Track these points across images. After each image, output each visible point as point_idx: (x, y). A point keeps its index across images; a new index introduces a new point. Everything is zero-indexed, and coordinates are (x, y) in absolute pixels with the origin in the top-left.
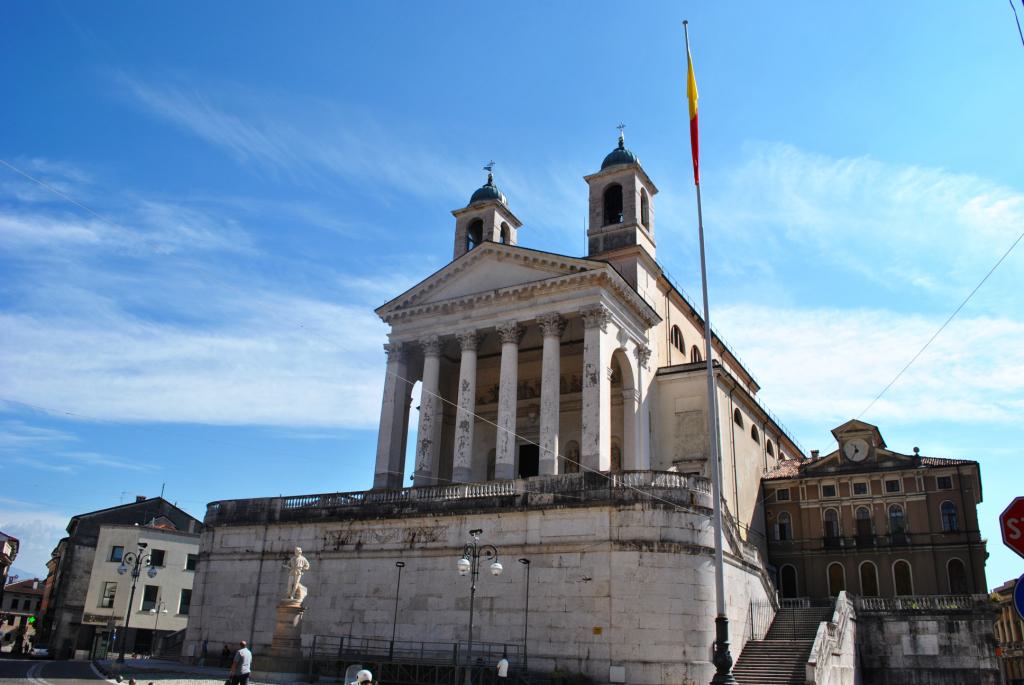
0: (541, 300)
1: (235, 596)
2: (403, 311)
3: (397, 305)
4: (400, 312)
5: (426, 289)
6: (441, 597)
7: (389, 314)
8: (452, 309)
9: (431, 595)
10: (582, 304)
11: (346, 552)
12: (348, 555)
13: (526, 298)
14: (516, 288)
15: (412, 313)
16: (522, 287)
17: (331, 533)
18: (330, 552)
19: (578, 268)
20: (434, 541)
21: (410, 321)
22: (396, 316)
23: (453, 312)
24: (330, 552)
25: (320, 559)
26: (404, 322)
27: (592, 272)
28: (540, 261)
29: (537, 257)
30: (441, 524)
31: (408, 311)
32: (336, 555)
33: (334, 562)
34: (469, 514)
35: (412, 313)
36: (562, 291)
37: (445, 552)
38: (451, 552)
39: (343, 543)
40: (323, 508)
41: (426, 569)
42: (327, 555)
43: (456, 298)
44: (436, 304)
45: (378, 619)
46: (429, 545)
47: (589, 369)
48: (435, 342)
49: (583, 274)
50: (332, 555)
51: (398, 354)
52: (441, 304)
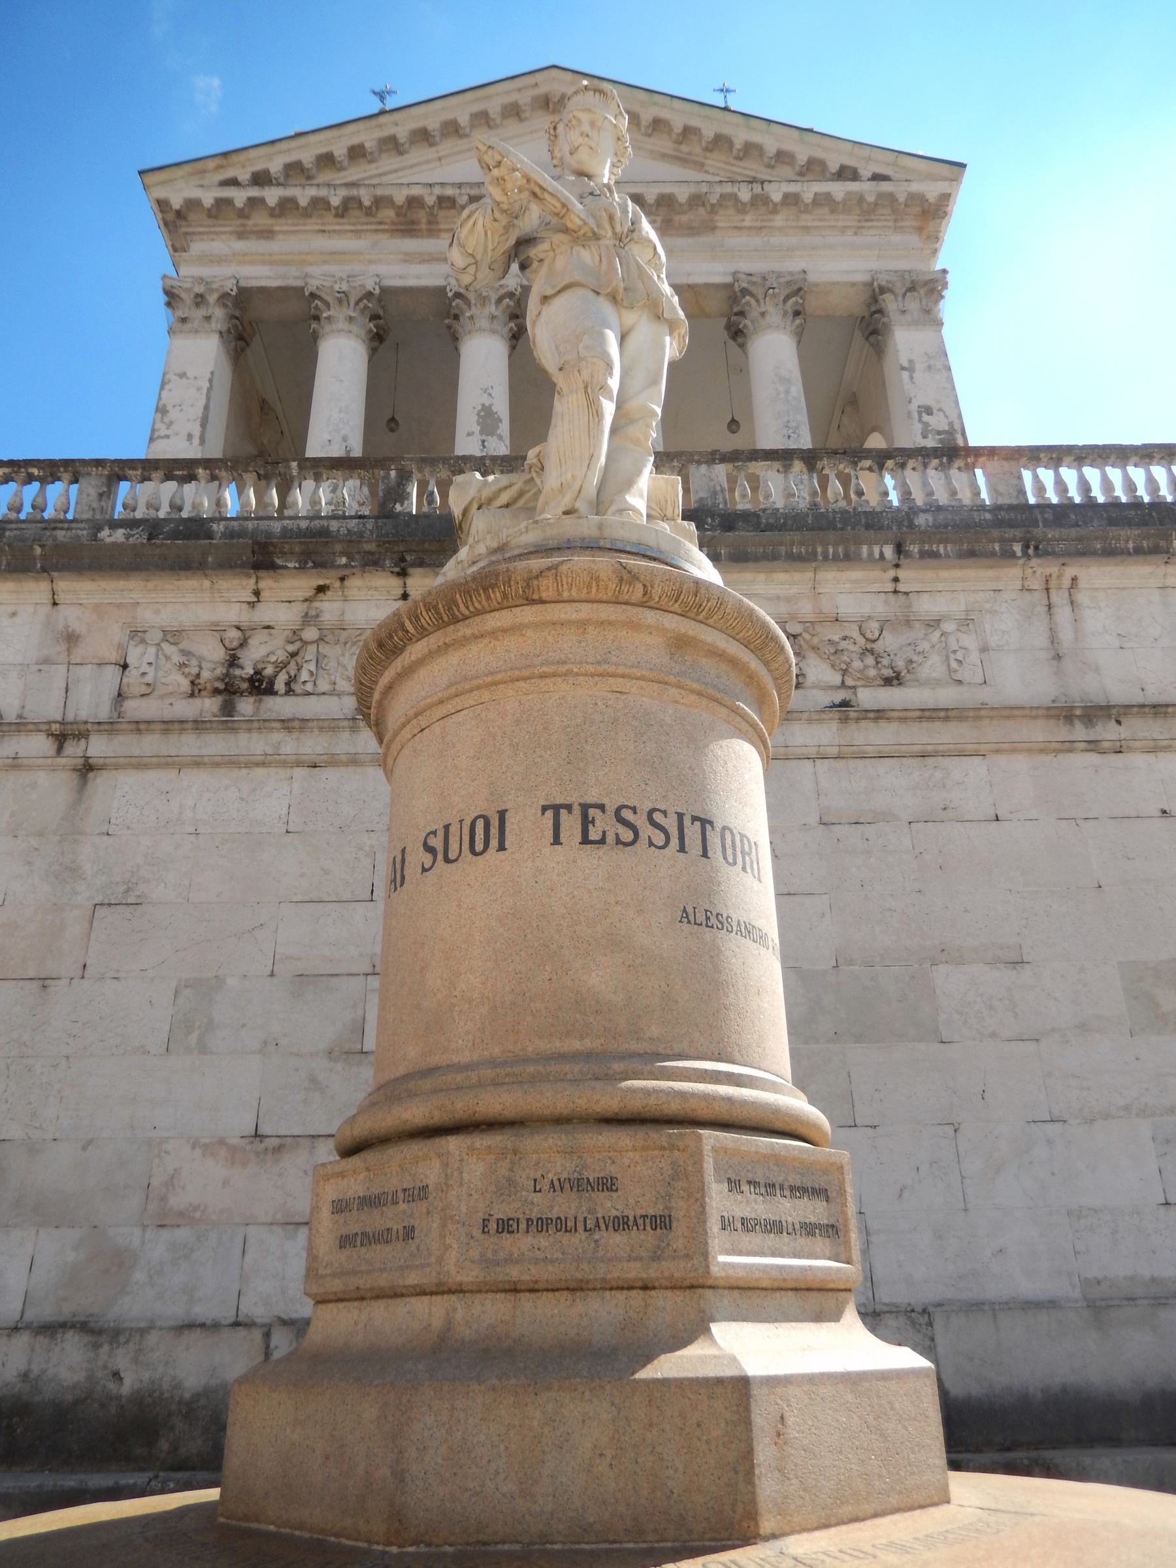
0: (737, 241)
2: (254, 192)
3: (229, 174)
4: (239, 197)
5: (340, 151)
6: (1018, 963)
7: (195, 193)
8: (432, 221)
9: (946, 954)
10: (874, 265)
11: (287, 724)
12: (313, 745)
13: (692, 230)
14: (668, 189)
15: (286, 207)
16: (693, 189)
17: (172, 635)
18: (169, 726)
19: (866, 173)
20: (893, 680)
21: (267, 234)
22: (223, 204)
23: (433, 231)
24: (169, 726)
25: (87, 769)
26: (241, 235)
27: (915, 187)
28: (738, 144)
29: (727, 131)
30: (926, 606)
31: (272, 195)
32: (216, 744)
33: (196, 780)
34: (1110, 553)
35: (286, 207)
36: (806, 229)
37: (993, 732)
38: (1038, 732)
39: (260, 686)
40: (114, 525)
41: (886, 816)
42: (150, 744)
43: (460, 186)
44: (379, 192)
46: (868, 697)
47: (926, 418)
48: (369, 295)
49: (885, 187)
50: (189, 744)
51: (219, 313)
52: (400, 197)
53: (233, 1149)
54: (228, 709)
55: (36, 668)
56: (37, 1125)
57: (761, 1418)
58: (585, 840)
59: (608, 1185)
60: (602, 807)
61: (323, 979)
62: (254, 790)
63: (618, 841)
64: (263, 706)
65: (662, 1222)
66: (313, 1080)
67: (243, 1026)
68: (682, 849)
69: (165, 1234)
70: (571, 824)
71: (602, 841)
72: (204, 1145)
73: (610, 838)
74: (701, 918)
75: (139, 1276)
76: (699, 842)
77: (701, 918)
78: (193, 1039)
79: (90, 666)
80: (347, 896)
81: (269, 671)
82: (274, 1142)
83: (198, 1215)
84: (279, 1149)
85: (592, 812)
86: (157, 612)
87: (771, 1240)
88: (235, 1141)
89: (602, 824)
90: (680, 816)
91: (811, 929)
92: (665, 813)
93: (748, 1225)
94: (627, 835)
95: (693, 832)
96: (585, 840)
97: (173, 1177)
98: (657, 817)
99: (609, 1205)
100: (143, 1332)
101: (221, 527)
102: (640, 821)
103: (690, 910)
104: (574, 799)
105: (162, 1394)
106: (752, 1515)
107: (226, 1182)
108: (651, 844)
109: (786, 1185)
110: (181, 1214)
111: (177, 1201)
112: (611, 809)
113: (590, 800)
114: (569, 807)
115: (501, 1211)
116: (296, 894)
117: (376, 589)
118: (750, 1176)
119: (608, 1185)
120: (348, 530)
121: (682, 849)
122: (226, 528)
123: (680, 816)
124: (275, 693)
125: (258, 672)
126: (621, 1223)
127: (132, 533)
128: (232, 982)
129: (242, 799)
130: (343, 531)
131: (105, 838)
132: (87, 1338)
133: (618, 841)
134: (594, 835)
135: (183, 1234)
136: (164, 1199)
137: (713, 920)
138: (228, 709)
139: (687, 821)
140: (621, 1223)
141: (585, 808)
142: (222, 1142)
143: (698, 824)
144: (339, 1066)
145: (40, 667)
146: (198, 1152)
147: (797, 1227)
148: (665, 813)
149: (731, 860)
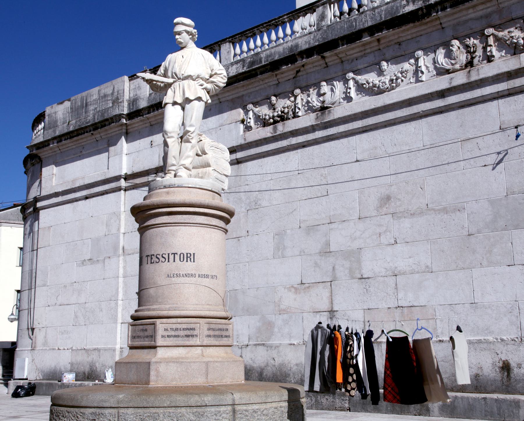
1: (83, 262)
45: (402, 265)
53: (296, 289)
54: (275, 129)
55: (219, 128)
56: (244, 284)
57: (152, 367)
58: (151, 263)
59: (146, 330)
60: (154, 255)
61: (315, 227)
62: (287, 159)
63: (156, 262)
64: (286, 125)
65: (152, 336)
66: (316, 263)
67: (294, 247)
68: (169, 261)
69: (281, 316)
70: (149, 258)
71: (153, 263)
72: (288, 288)
73: (155, 262)
74: (172, 276)
75: (276, 330)
76: (173, 259)
77: (172, 276)
78: (280, 253)
79: (234, 124)
80: (319, 195)
81: (286, 110)
82: (307, 285)
83: (289, 310)
84: (309, 287)
85: (152, 256)
86: (249, 97)
87: (175, 339)
88: (296, 286)
89: (154, 259)
90: (169, 254)
91: (495, 180)
92: (165, 254)
93: (168, 336)
94: (158, 261)
95: (172, 257)
96: (151, 263)
97: (280, 299)
98: (164, 256)
99: (146, 334)
100: (278, 347)
101: (264, 54)
102: (160, 257)
103: (169, 275)
104: (150, 254)
105: (285, 365)
106: (149, 382)
107: (295, 300)
108: (162, 262)
109: (182, 328)
110: (284, 310)
111: (282, 307)
112: (155, 255)
113: (152, 254)
114: (149, 256)
115: (134, 335)
116: (303, 197)
117: (316, 66)
118: (171, 327)
119: (146, 330)
120: (305, 42)
121: (169, 261)
122: (266, 54)
123: (169, 254)
124: (289, 119)
125: (282, 112)
126: (147, 337)
127: (238, 66)
128: (288, 232)
129: (283, 164)
130: (304, 42)
131: (247, 186)
132: (266, 348)
133: (156, 262)
134: (152, 262)
135: (285, 316)
136: (279, 306)
137: (175, 276)
138: (275, 129)
139: (170, 255)
140: (147, 337)
141: (151, 255)
142: (292, 287)
143: (173, 255)
144: (323, 258)
145: (220, 128)
146: (286, 290)
147: (184, 336)
148: (165, 254)
149: (182, 260)
